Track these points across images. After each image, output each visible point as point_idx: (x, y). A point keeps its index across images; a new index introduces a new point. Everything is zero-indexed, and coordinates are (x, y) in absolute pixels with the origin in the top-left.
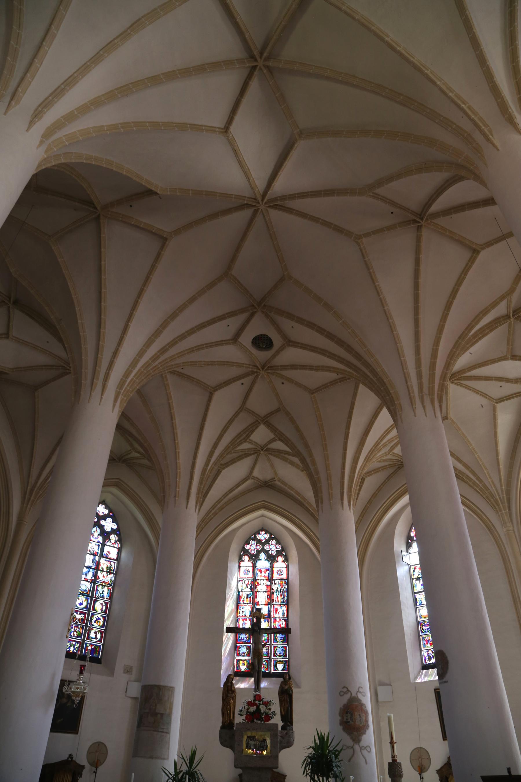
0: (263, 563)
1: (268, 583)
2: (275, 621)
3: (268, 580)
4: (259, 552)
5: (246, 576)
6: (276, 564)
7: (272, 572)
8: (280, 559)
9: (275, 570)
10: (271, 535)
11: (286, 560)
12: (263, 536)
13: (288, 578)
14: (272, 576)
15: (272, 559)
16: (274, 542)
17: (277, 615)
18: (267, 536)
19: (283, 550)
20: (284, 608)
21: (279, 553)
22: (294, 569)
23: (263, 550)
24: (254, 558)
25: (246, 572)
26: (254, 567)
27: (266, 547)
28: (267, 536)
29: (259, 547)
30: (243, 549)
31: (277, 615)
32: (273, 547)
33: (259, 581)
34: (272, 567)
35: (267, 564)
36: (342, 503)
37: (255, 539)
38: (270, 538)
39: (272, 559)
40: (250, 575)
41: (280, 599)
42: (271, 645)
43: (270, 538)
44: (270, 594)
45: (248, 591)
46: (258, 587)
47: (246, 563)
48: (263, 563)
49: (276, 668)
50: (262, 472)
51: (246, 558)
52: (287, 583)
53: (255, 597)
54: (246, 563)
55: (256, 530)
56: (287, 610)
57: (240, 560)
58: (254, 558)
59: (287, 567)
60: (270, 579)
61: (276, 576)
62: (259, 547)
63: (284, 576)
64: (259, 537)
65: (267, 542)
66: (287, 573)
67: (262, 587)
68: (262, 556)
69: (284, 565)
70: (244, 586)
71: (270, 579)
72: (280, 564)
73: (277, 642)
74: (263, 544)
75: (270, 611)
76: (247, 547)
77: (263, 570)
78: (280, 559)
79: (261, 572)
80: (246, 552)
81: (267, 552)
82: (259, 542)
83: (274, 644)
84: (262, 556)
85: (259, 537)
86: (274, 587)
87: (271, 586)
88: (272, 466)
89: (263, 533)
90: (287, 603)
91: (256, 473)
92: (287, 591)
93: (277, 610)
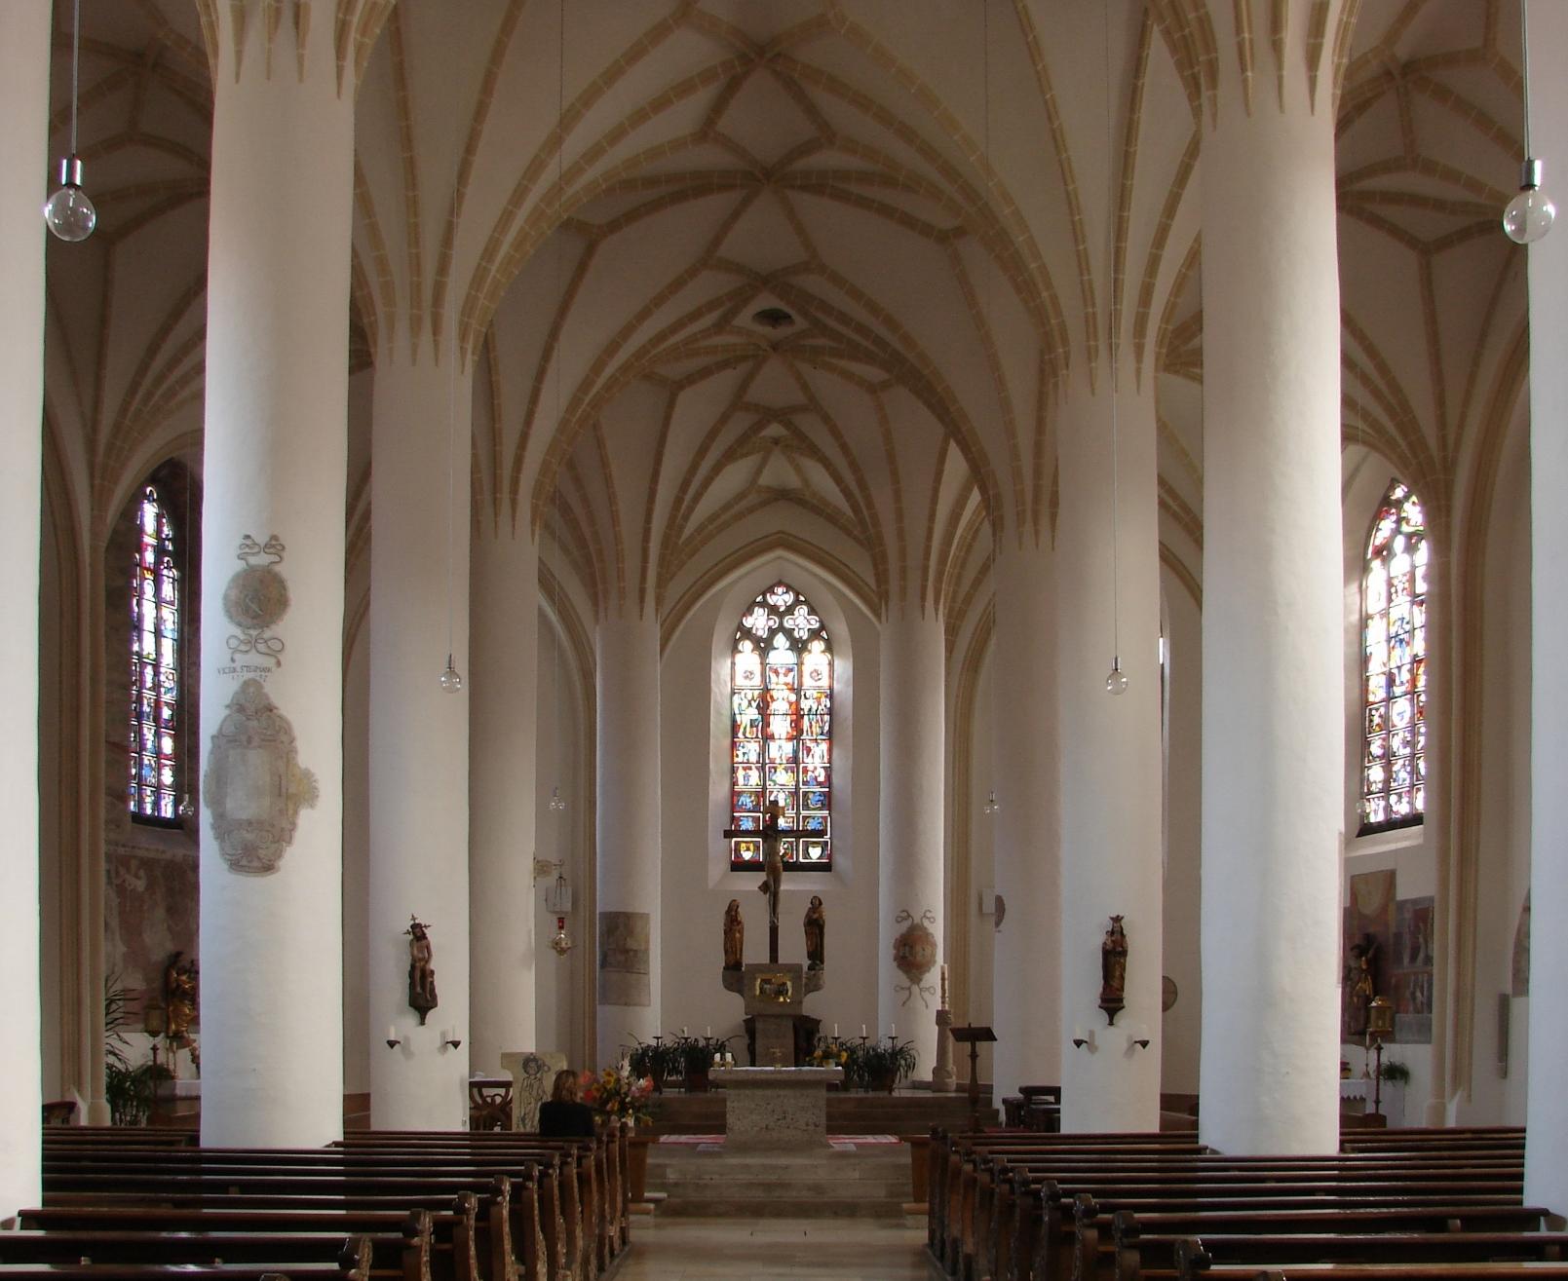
0: (781, 654)
1: (793, 697)
2: (805, 771)
3: (792, 689)
4: (773, 632)
5: (747, 683)
6: (806, 656)
7: (800, 676)
8: (817, 646)
9: (807, 669)
10: (797, 594)
11: (829, 648)
12: (781, 598)
13: (831, 688)
14: (801, 684)
15: (799, 647)
16: (804, 610)
17: (808, 760)
18: (790, 598)
19: (823, 627)
20: (824, 746)
21: (815, 634)
22: (844, 667)
23: (781, 628)
24: (764, 646)
25: (749, 675)
26: (763, 664)
27: (788, 623)
28: (790, 598)
29: (774, 623)
30: (741, 627)
31: (808, 760)
32: (802, 621)
33: (774, 693)
34: (800, 664)
35: (790, 658)
36: (923, 607)
37: (764, 604)
38: (797, 602)
39: (799, 647)
40: (757, 681)
41: (816, 729)
42: (798, 814)
43: (797, 602)
44: (797, 716)
45: (753, 713)
46: (773, 706)
47: (747, 652)
48: (781, 654)
49: (807, 854)
50: (779, 471)
51: (747, 646)
52: (831, 696)
53: (766, 724)
54: (747, 652)
55: (769, 583)
56: (830, 751)
57: (735, 650)
58: (764, 646)
59: (831, 664)
60: (797, 690)
61: (807, 682)
62: (774, 623)
63: (825, 683)
64: (772, 600)
65: (790, 610)
66: (831, 677)
67: (780, 704)
68: (780, 640)
69: (826, 658)
70: (745, 703)
71: (797, 690)
72: (817, 656)
73: (807, 807)
74: (781, 616)
75: (796, 752)
76: (748, 622)
77: (782, 671)
78: (817, 646)
79: (776, 672)
80: (748, 634)
81: (789, 633)
82: (773, 610)
83: (804, 813)
84: (780, 640)
85: (772, 600)
86: (805, 705)
87: (798, 702)
88: (799, 470)
89: (780, 590)
90: (830, 736)
91: (765, 480)
92: (831, 712)
93: (809, 750)
